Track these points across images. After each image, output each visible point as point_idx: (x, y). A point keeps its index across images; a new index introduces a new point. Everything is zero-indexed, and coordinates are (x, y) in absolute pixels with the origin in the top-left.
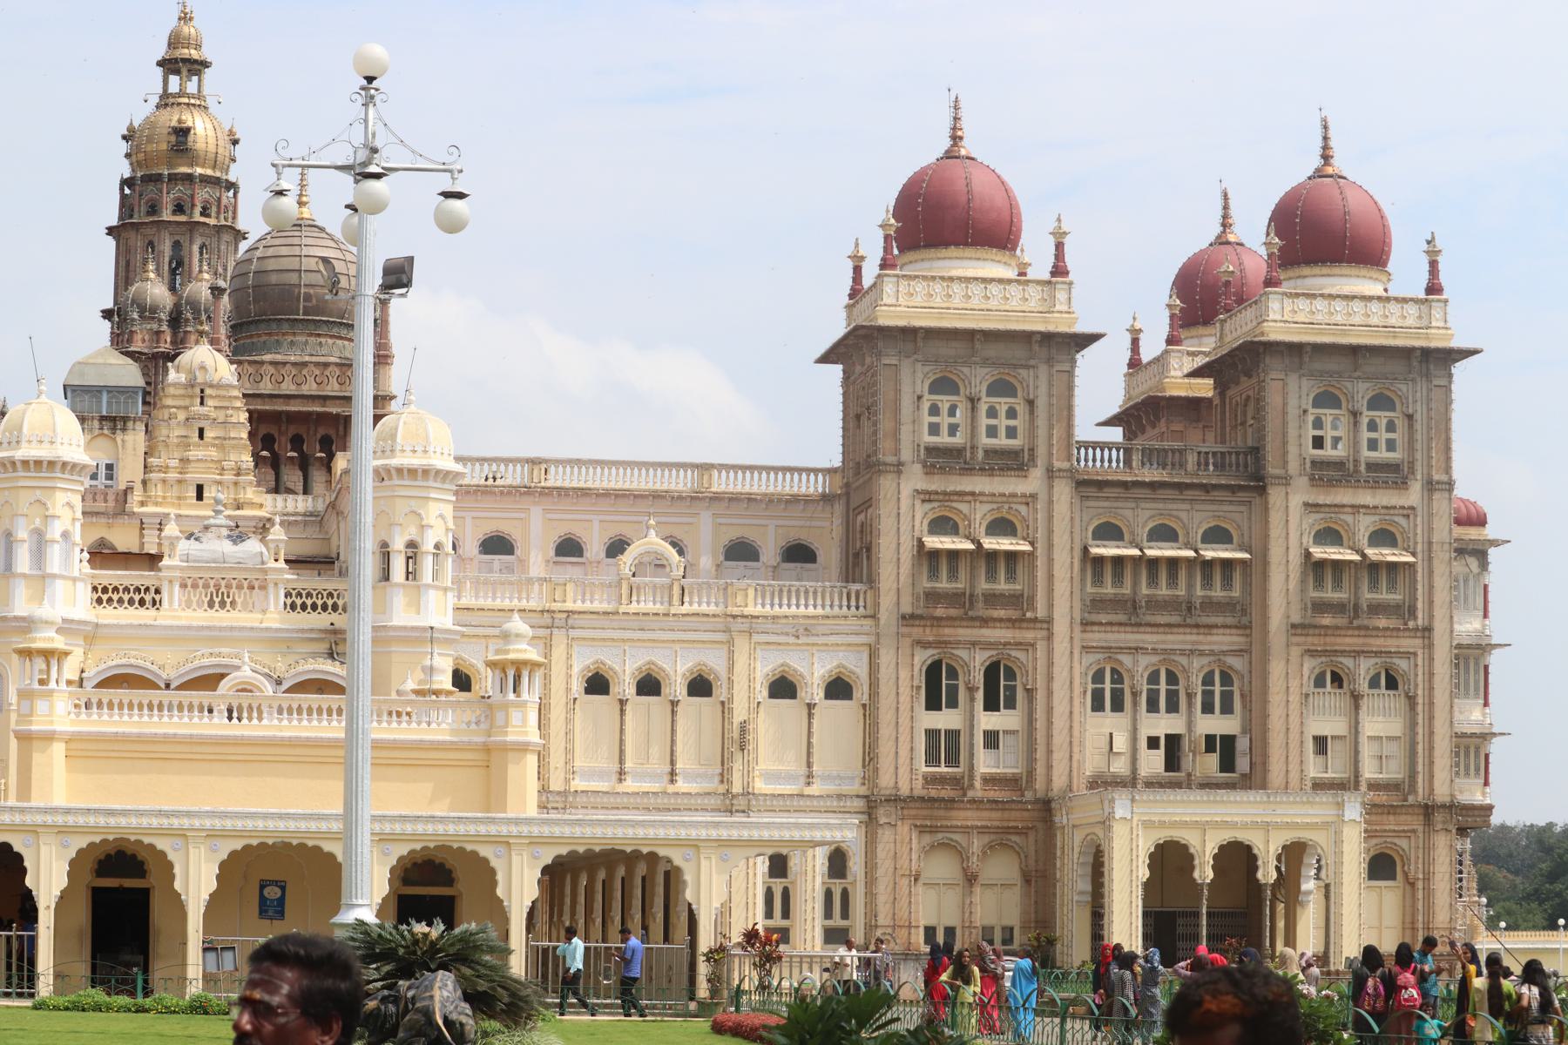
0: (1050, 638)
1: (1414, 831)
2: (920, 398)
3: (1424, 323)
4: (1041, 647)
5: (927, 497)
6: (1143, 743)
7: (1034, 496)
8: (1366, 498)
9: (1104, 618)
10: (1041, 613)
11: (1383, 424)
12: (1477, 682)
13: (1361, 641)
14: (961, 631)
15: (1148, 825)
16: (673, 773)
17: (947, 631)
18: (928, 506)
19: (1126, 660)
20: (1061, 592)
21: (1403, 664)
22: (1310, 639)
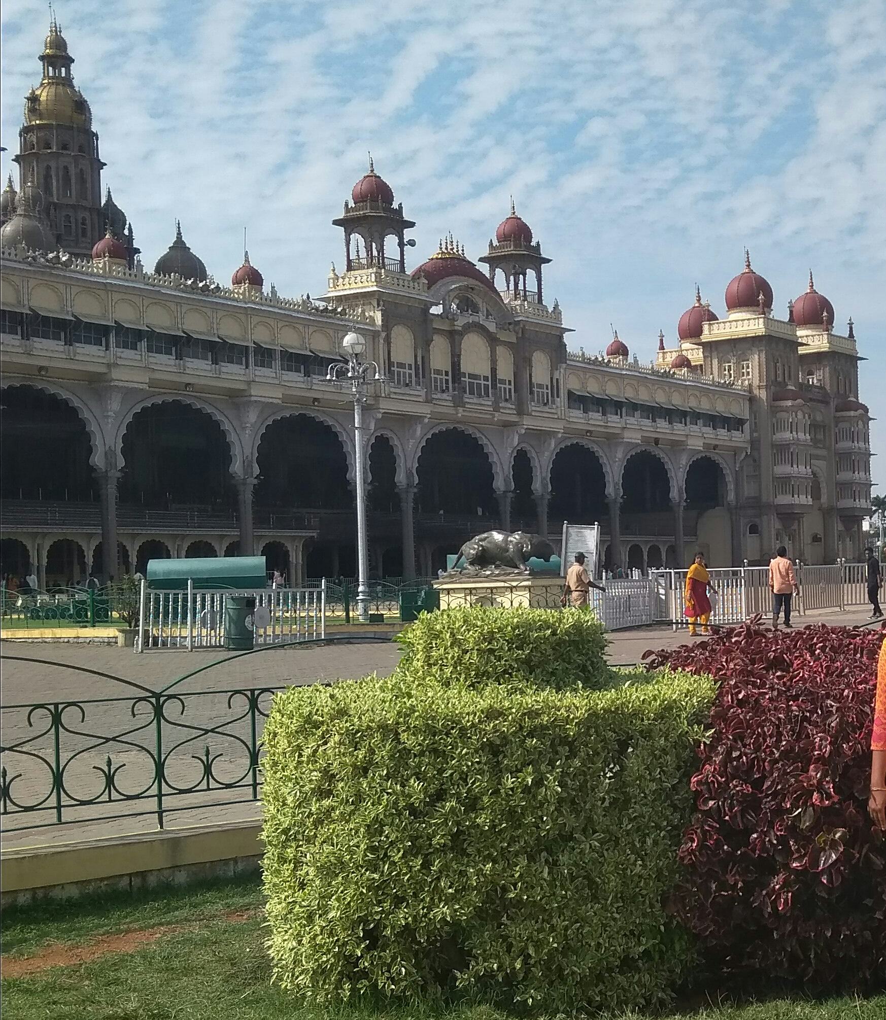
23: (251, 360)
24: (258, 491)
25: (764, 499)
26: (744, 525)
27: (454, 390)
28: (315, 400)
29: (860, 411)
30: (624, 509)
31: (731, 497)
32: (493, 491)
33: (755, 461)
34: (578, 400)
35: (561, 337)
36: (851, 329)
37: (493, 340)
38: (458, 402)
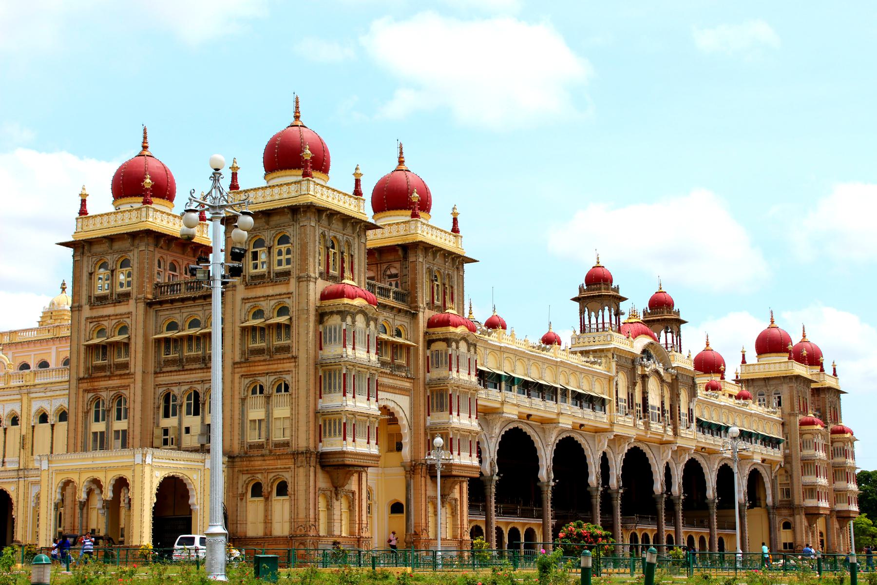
0: (134, 382)
1: (289, 468)
2: (91, 274)
3: (299, 193)
4: (132, 385)
5: (90, 320)
6: (184, 430)
7: (129, 313)
8: (270, 291)
9: (169, 369)
10: (132, 371)
11: (284, 251)
12: (340, 384)
13: (266, 367)
14: (102, 383)
15: (60, 472)
16: (3, 462)
17: (96, 384)
18: (92, 325)
19: (175, 390)
20: (137, 359)
21: (288, 378)
22: (243, 369)
23: (559, 396)
24: (555, 490)
25: (796, 502)
26: (779, 521)
27: (645, 417)
28: (582, 425)
29: (848, 435)
30: (718, 508)
31: (769, 500)
32: (653, 492)
33: (786, 472)
34: (703, 426)
35: (693, 379)
36: (834, 369)
37: (662, 380)
38: (647, 425)
